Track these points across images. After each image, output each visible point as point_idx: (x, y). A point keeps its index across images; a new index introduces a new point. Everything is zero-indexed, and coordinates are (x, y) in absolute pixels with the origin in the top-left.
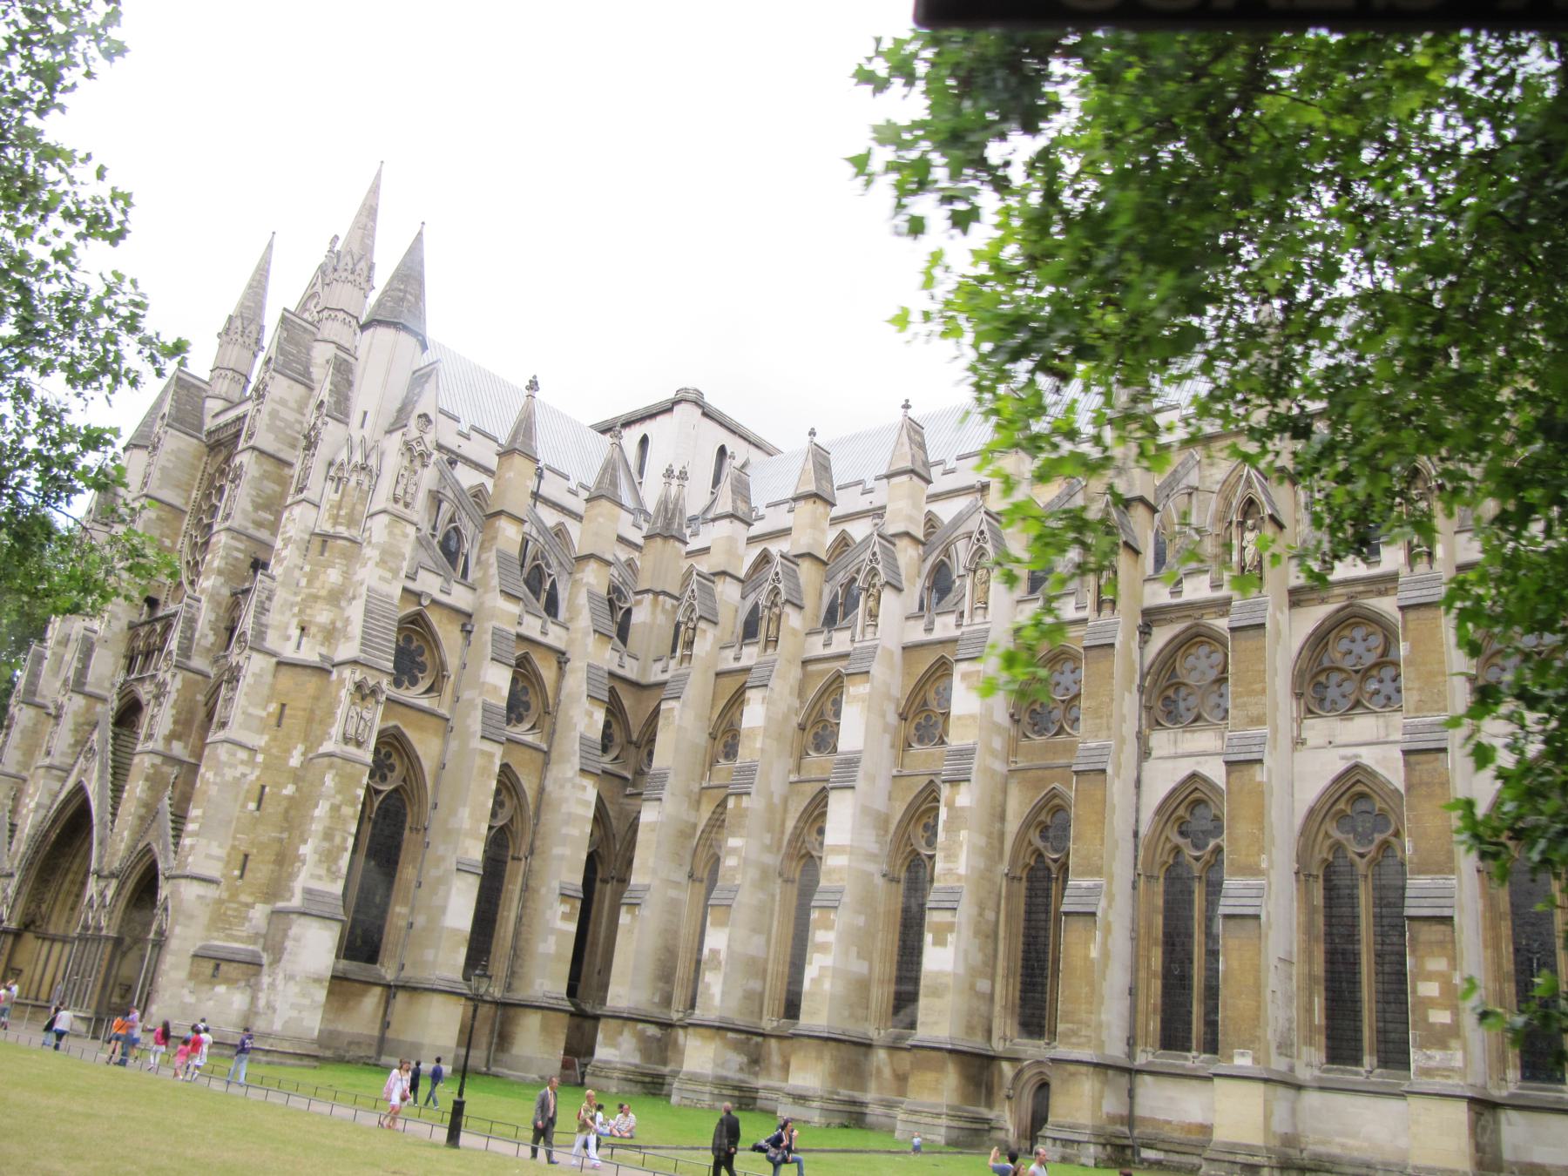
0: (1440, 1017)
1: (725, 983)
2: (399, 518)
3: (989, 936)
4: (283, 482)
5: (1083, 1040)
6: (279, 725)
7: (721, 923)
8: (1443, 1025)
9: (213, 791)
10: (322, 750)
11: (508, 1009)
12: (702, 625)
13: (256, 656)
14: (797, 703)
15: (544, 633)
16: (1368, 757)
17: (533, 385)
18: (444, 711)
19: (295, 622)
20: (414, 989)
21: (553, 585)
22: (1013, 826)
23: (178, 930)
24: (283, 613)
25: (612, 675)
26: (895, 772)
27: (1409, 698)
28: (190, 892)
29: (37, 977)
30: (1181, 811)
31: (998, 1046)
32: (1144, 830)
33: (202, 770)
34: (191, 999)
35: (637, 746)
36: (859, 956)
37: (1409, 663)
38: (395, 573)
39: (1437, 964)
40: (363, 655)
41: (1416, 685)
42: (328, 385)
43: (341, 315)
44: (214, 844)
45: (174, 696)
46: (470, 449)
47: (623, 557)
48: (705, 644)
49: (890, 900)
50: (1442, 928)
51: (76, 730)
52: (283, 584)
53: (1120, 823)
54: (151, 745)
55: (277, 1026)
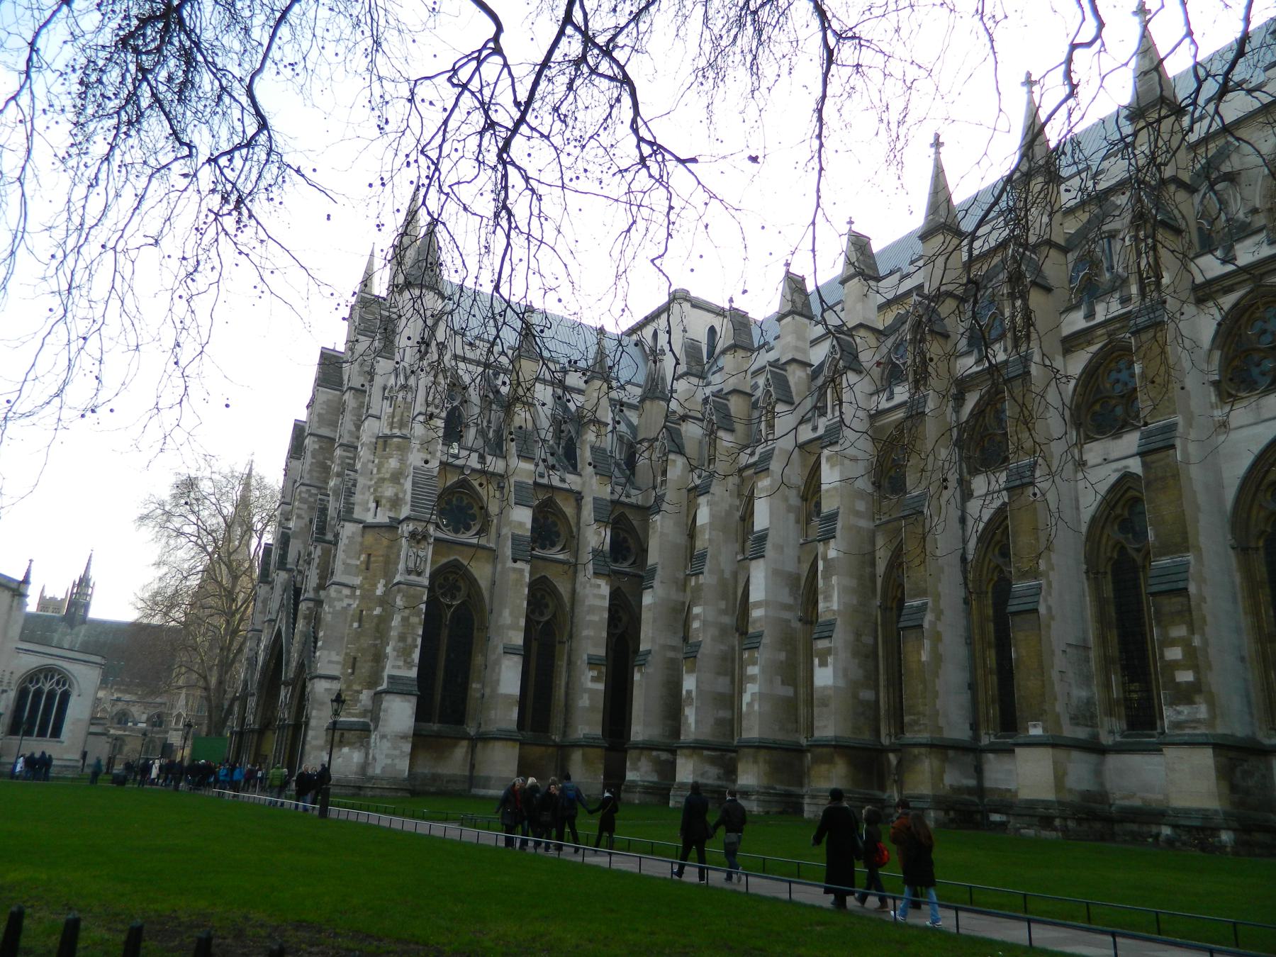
0: (1185, 676)
1: (697, 714)
5: (922, 727)
7: (691, 671)
8: (1187, 683)
10: (395, 581)
11: (564, 749)
13: (347, 524)
14: (737, 502)
18: (492, 545)
19: (372, 498)
20: (485, 738)
23: (314, 713)
24: (364, 494)
26: (801, 541)
31: (885, 741)
32: (970, 557)
36: (783, 683)
39: (1179, 631)
45: (317, 561)
50: (1180, 599)
55: (378, 771)
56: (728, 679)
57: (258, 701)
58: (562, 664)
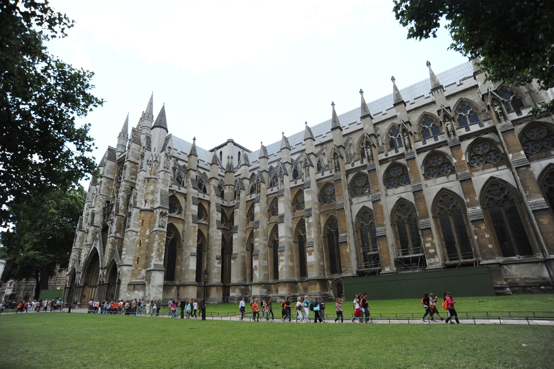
0: (432, 251)
2: (166, 172)
3: (321, 252)
4: (137, 168)
6: (142, 225)
7: (257, 259)
9: (128, 243)
10: (154, 230)
12: (241, 190)
13: (134, 209)
14: (267, 205)
15: (204, 197)
16: (403, 196)
17: (194, 139)
18: (182, 218)
19: (143, 200)
20: (185, 286)
21: (205, 186)
22: (323, 225)
23: (123, 279)
25: (222, 205)
27: (412, 180)
28: (125, 269)
29: (90, 297)
30: (362, 215)
31: (327, 277)
32: (354, 221)
33: (125, 239)
34: (128, 295)
35: (229, 221)
37: (410, 172)
38: (167, 185)
39: (429, 239)
40: (161, 206)
41: (413, 177)
42: (145, 143)
43: (146, 128)
44: (130, 256)
45: (116, 222)
46: (181, 157)
47: (220, 179)
48: (243, 194)
49: (295, 247)
51: (92, 235)
52: (139, 191)
53: (349, 220)
54: (111, 235)
56: (267, 261)
57: (83, 274)
58: (205, 258)
